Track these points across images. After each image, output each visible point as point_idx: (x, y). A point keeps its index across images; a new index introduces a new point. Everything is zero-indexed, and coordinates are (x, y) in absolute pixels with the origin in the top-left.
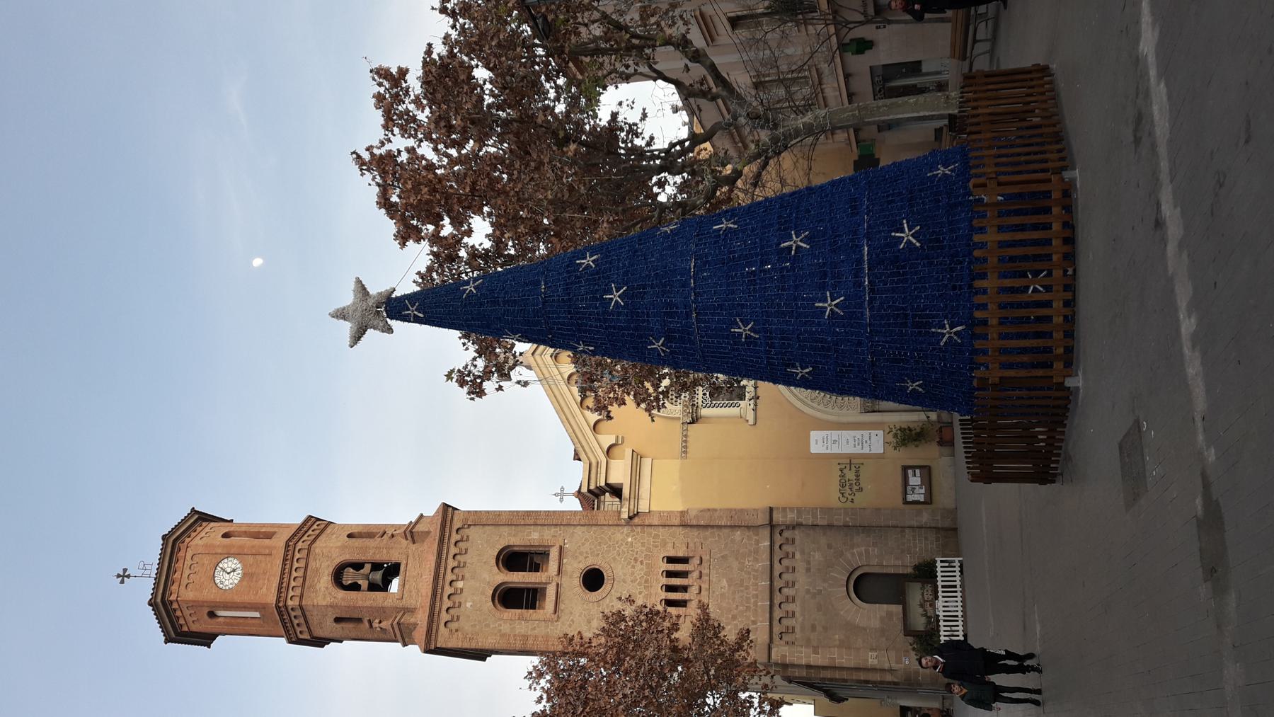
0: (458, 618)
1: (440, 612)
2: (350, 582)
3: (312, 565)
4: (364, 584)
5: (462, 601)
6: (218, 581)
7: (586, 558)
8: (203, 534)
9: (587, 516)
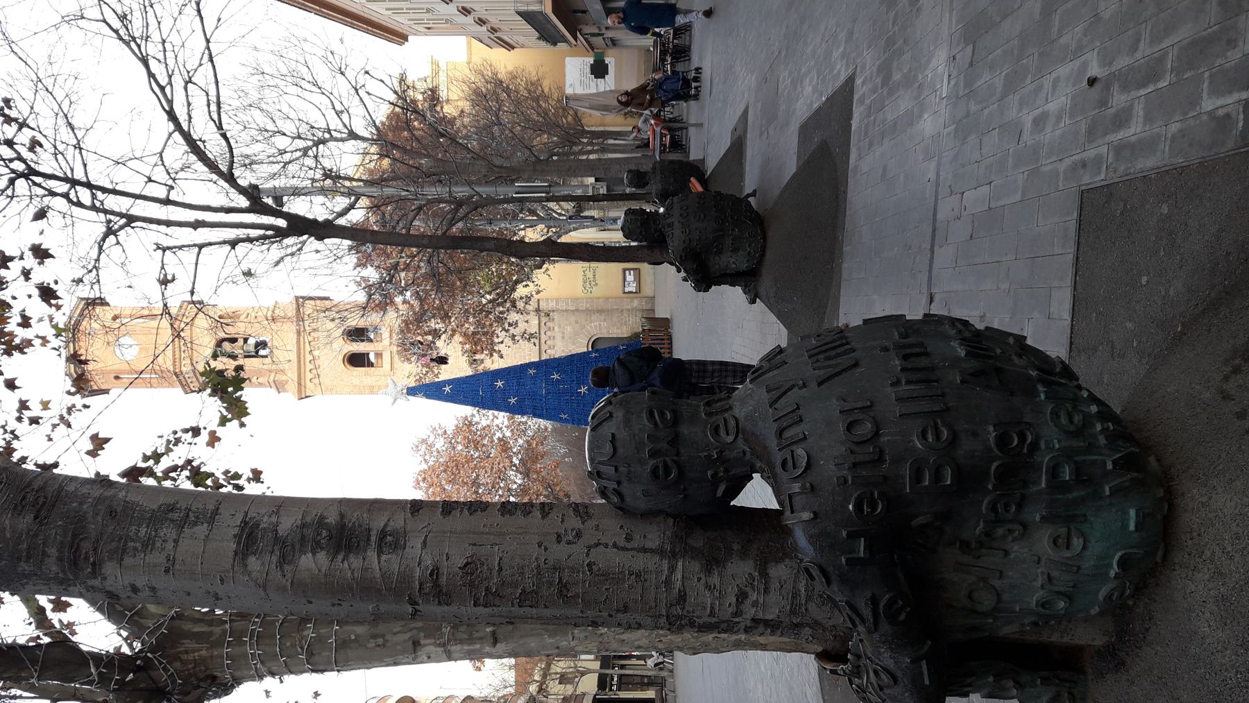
1: (305, 372)
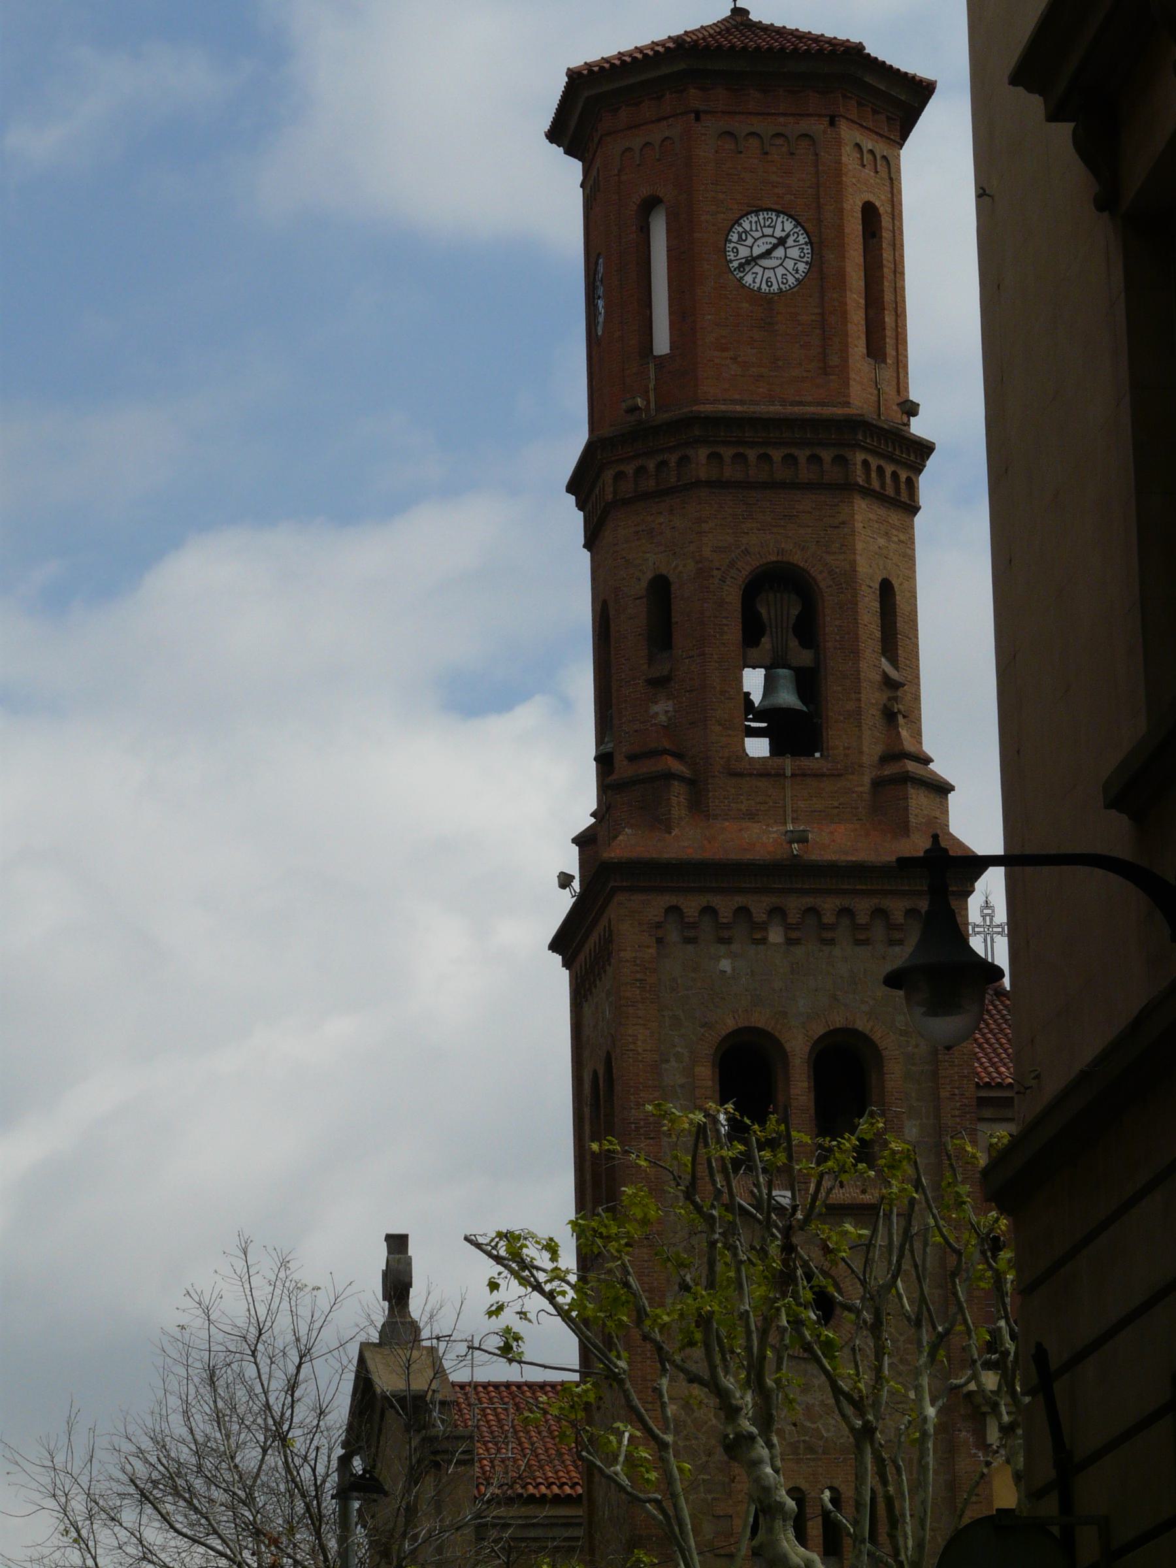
2: (763, 611)
5: (735, 947)
6: (746, 225)
8: (868, 145)
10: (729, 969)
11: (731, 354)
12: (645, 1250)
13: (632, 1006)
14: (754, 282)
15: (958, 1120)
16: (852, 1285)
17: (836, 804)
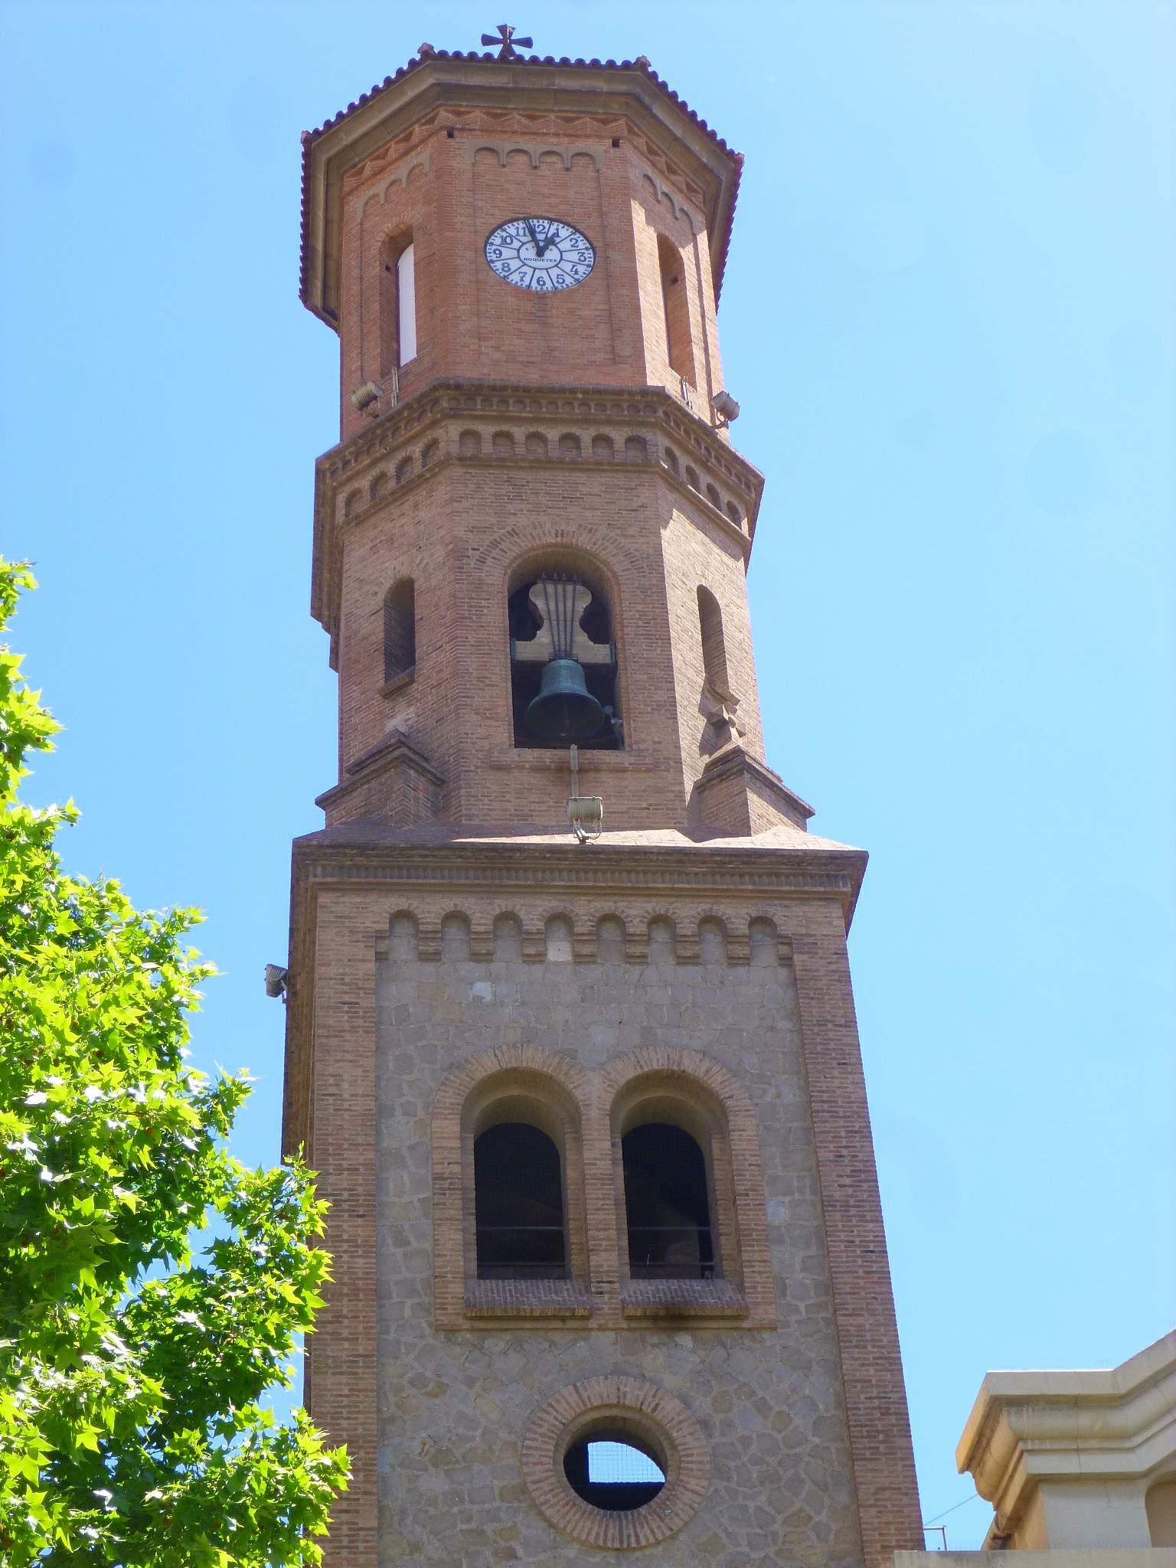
0: (434, 957)
2: (540, 604)
3: (593, 485)
4: (538, 647)
5: (497, 966)
7: (705, 1424)
8: (663, 186)
9: (886, 1413)
10: (488, 998)
11: (492, 343)
12: (344, 1379)
13: (336, 1036)
14: (522, 280)
15: (850, 1191)
16: (691, 1434)
17: (644, 805)
